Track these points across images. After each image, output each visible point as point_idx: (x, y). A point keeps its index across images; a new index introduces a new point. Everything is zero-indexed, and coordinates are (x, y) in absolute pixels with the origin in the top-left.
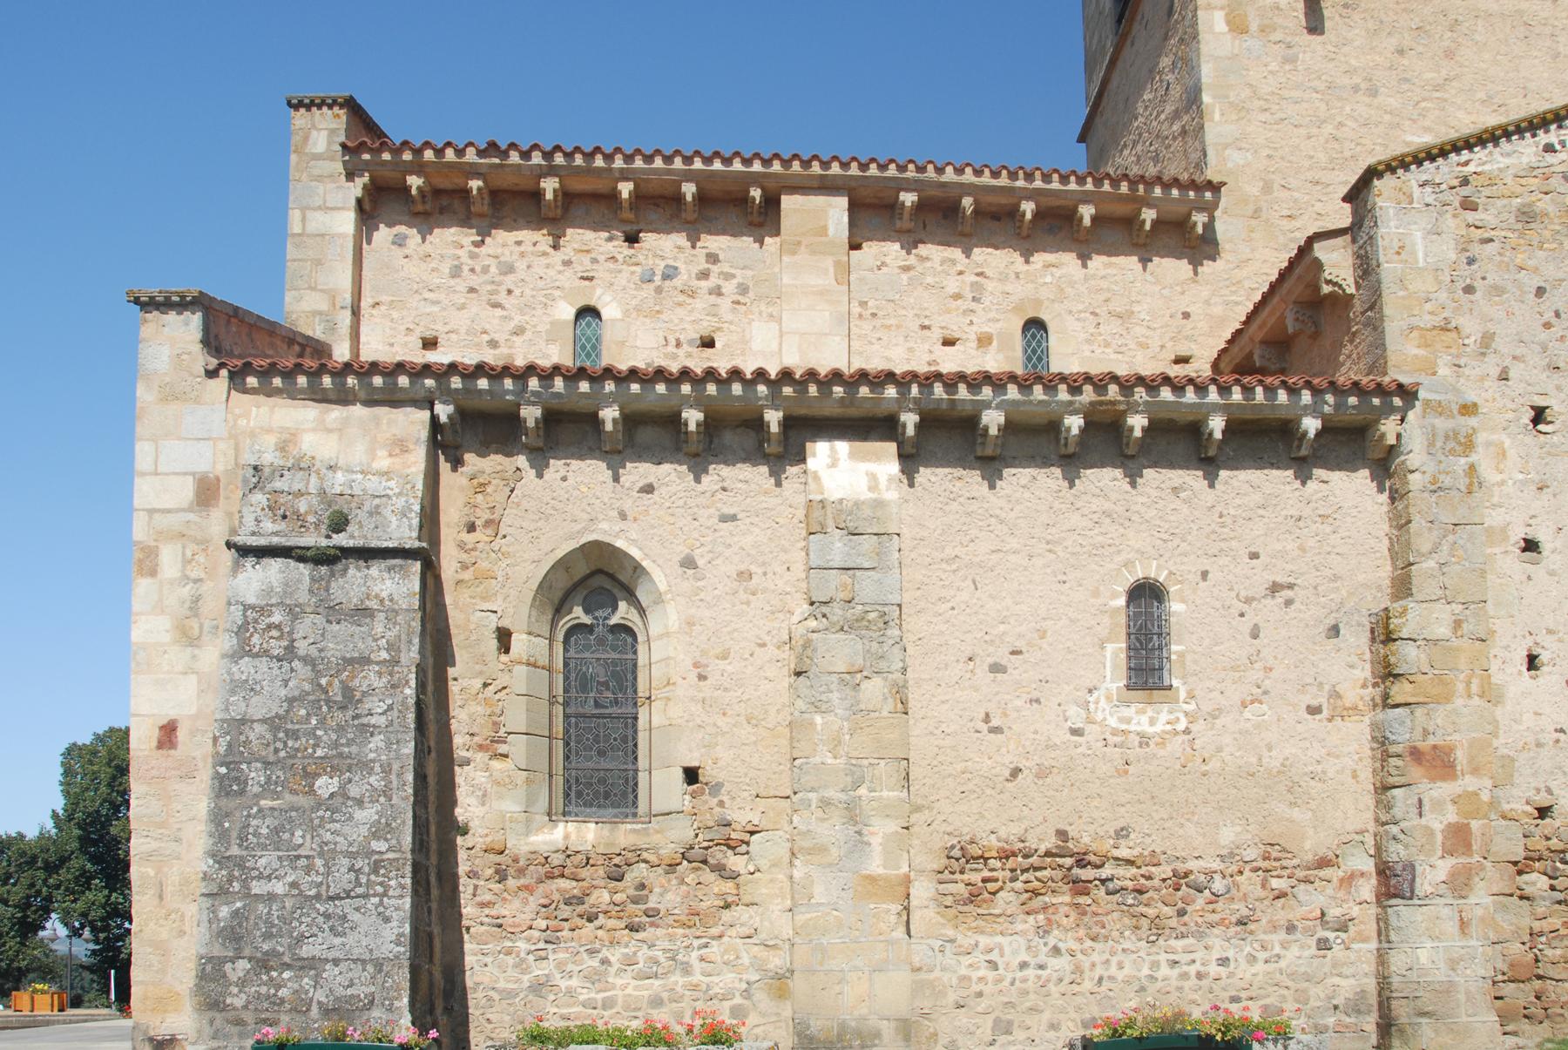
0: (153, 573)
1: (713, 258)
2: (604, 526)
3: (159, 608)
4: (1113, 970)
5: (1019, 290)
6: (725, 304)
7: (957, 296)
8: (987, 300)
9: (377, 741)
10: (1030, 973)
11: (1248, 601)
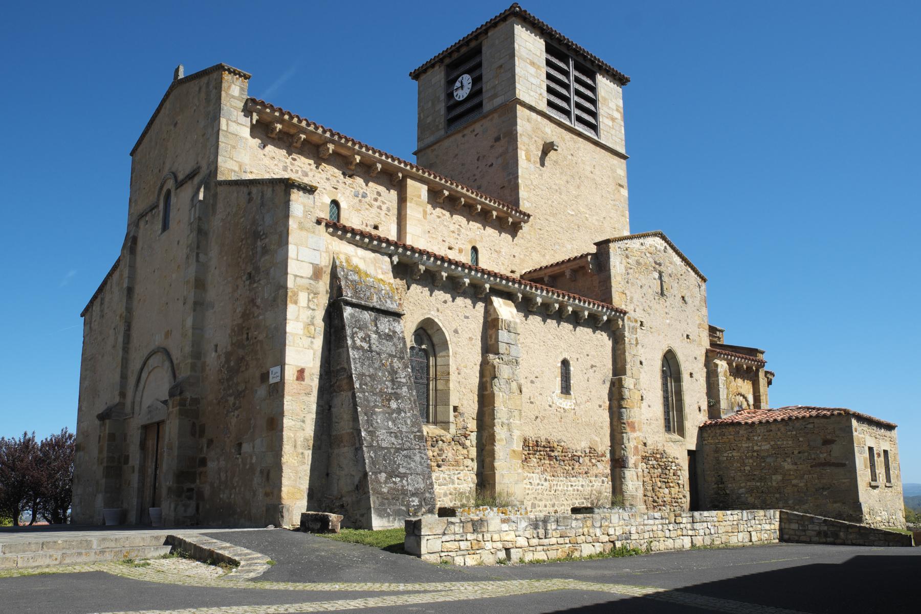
0: (296, 303)
1: (379, 194)
3: (297, 319)
5: (471, 235)
6: (383, 213)
7: (453, 232)
9: (405, 389)
10: (540, 487)
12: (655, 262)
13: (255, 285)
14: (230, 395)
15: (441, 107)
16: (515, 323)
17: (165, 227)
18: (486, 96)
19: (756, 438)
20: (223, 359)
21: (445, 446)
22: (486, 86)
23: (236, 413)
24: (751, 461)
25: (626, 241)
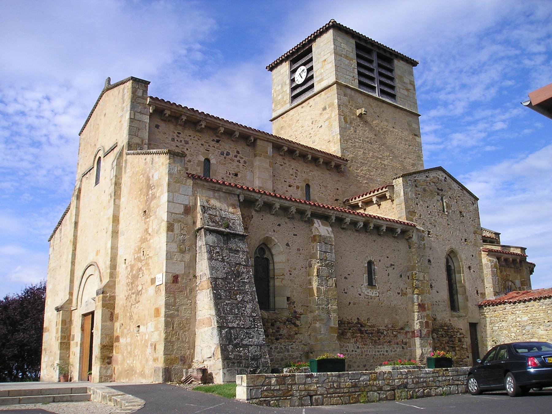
2: (270, 233)
4: (368, 353)
5: (305, 176)
6: (241, 165)
7: (292, 175)
8: (298, 177)
10: (354, 353)
11: (387, 267)
12: (438, 189)
13: (148, 220)
14: (133, 293)
15: (287, 89)
16: (330, 237)
17: (97, 182)
18: (315, 80)
19: (518, 312)
20: (129, 269)
21: (281, 325)
22: (316, 72)
23: (137, 305)
24: (515, 329)
25: (414, 175)
